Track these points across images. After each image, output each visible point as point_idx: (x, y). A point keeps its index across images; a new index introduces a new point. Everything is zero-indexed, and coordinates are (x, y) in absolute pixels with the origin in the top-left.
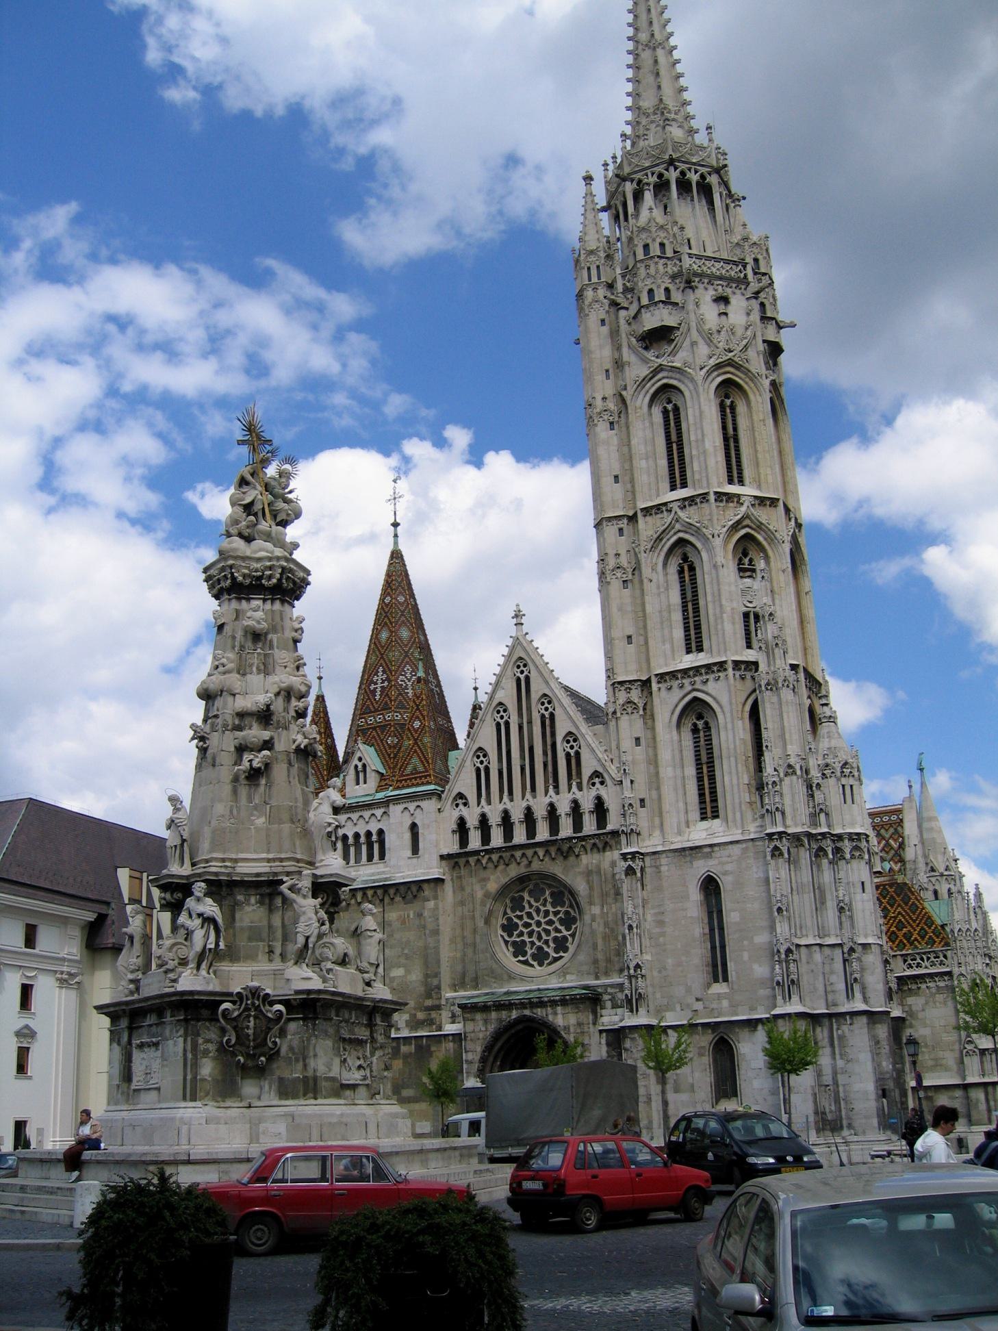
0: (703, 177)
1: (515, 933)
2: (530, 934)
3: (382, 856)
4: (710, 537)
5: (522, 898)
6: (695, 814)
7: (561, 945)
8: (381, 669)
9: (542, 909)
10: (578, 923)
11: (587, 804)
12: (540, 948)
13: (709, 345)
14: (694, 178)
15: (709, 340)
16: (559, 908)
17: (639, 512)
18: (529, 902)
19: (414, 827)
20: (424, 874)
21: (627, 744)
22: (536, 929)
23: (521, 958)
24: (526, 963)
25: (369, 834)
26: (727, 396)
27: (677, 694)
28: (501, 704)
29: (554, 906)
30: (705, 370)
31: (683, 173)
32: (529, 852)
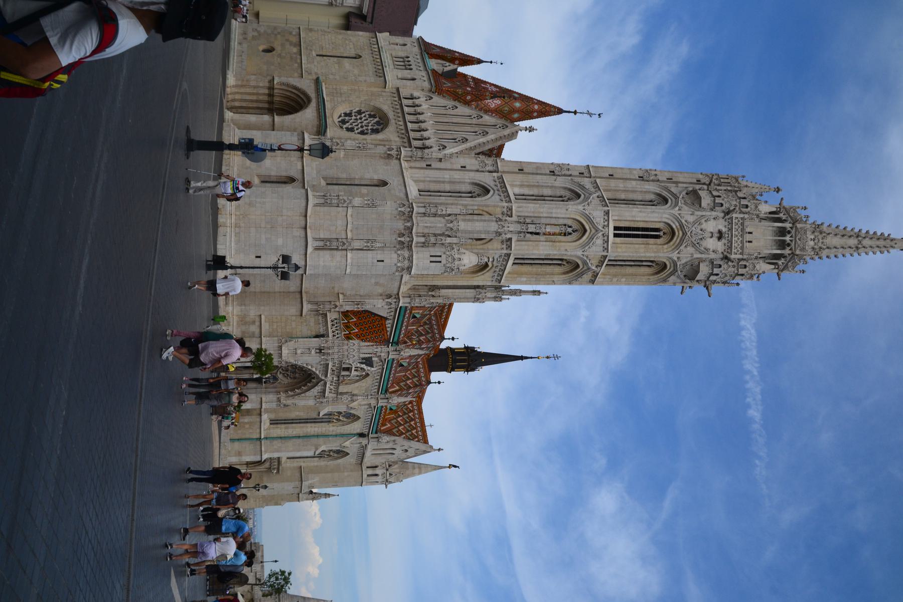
0: (789, 245)
4: (583, 205)
5: (376, 118)
6: (422, 187)
8: (498, 90)
9: (370, 124)
12: (348, 122)
13: (693, 222)
14: (787, 238)
15: (694, 223)
18: (373, 120)
20: (388, 79)
22: (359, 121)
23: (343, 115)
24: (340, 116)
25: (410, 65)
26: (664, 234)
29: (371, 129)
30: (678, 216)
31: (789, 232)
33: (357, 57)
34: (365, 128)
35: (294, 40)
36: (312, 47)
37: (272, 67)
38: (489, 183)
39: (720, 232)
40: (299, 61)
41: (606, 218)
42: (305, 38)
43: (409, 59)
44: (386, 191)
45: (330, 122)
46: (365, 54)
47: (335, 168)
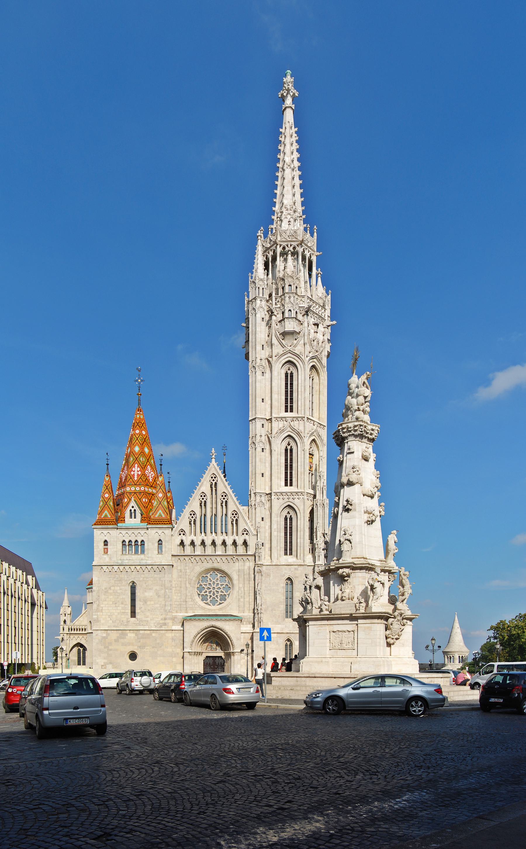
1: (203, 591)
2: (210, 592)
3: (143, 552)
4: (303, 437)
7: (223, 598)
10: (231, 590)
11: (240, 541)
16: (223, 583)
17: (273, 418)
19: (160, 542)
21: (259, 519)
23: (205, 601)
25: (136, 541)
27: (281, 501)
28: (203, 493)
32: (213, 558)
33: (131, 584)
34: (219, 586)
35: (114, 635)
36: (122, 621)
37: (159, 652)
38: (282, 504)
39: (315, 324)
40: (149, 632)
41: (310, 421)
42: (108, 626)
43: (127, 541)
44: (297, 579)
45: (221, 611)
46: (128, 577)
47: (274, 612)
